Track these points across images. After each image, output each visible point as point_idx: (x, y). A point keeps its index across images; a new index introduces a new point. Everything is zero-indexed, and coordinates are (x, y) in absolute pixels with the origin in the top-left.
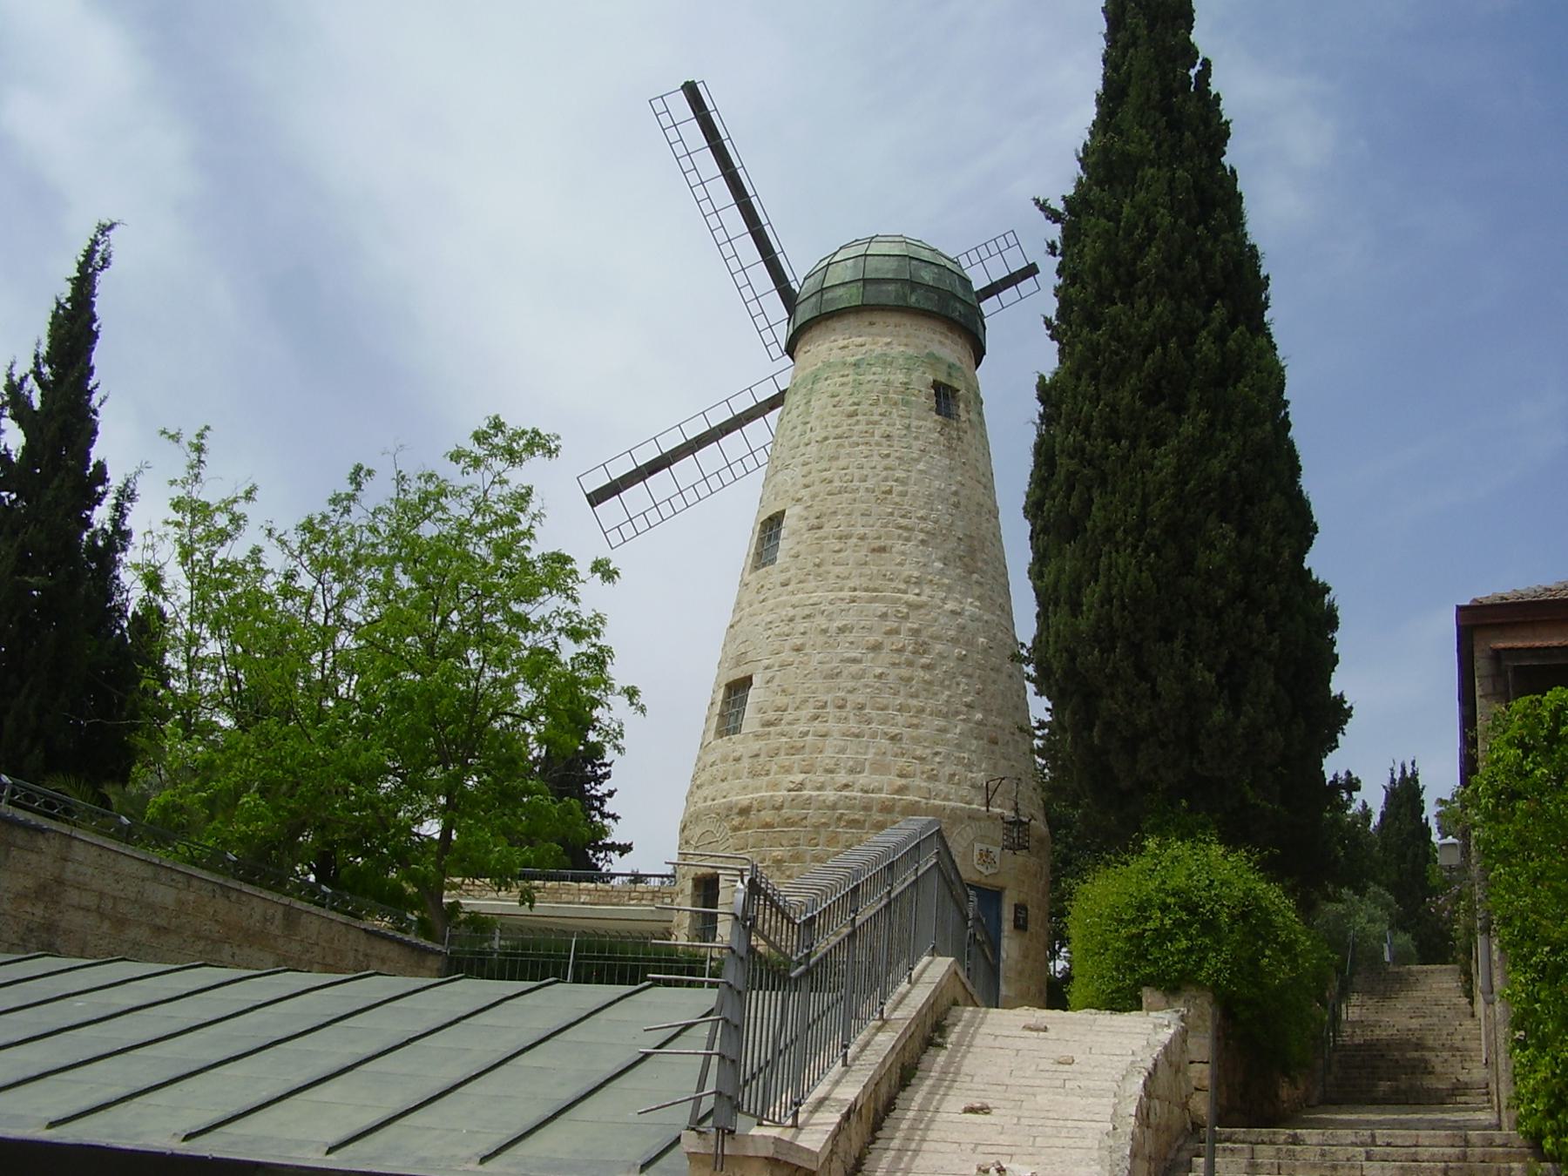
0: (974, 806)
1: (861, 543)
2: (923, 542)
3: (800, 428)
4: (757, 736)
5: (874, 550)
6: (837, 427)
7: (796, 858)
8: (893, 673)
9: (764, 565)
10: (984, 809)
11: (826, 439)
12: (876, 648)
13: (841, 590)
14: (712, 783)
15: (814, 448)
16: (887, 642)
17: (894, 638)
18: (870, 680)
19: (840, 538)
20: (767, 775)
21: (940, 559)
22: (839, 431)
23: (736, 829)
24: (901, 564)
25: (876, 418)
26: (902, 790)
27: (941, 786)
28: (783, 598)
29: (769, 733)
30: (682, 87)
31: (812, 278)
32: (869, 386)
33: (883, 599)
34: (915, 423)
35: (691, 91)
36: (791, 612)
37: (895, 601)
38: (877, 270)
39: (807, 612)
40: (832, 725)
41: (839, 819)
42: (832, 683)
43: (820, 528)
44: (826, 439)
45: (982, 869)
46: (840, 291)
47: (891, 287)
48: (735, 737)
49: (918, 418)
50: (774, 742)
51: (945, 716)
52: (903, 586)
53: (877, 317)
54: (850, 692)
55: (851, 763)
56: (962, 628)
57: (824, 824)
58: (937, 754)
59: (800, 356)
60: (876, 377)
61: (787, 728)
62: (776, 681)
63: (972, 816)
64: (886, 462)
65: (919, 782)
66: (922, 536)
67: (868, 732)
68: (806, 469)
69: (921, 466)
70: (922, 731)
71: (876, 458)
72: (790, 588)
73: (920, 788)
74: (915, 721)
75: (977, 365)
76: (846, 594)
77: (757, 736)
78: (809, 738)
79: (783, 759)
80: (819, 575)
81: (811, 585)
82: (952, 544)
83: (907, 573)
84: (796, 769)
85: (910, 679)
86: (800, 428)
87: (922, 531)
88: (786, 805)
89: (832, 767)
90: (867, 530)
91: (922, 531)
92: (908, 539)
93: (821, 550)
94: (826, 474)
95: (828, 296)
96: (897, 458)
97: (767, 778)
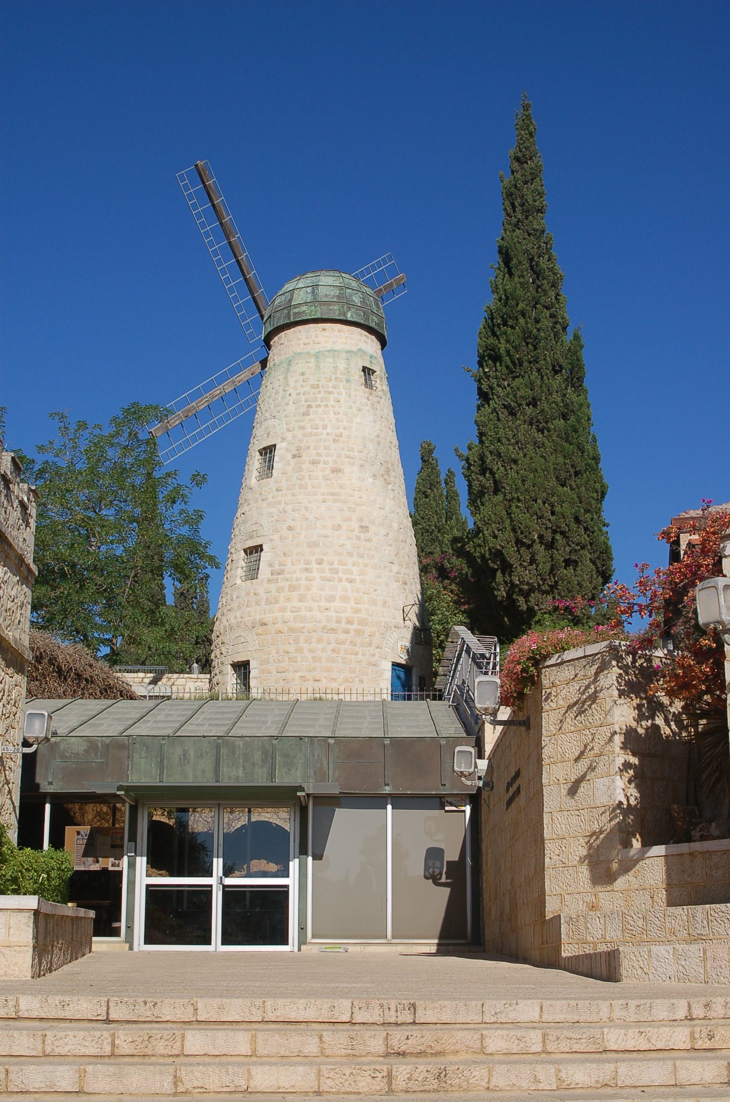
61: (288, 576)
69: (358, 420)
87: (360, 459)
92: (353, 464)
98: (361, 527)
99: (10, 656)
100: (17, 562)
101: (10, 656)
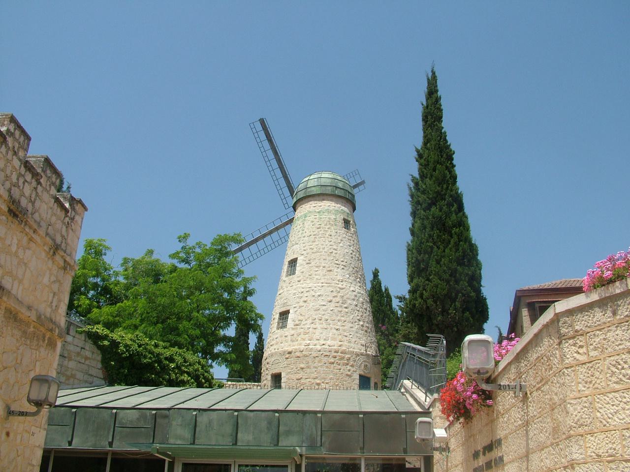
0: (362, 351)
1: (324, 268)
2: (343, 269)
3: (301, 232)
4: (293, 329)
5: (328, 271)
6: (313, 232)
7: (308, 367)
8: (336, 310)
9: (290, 275)
10: (365, 352)
11: (311, 235)
12: (330, 302)
13: (318, 283)
14: (277, 344)
15: (306, 238)
16: (334, 300)
17: (335, 298)
18: (329, 311)
19: (317, 267)
20: (297, 341)
21: (348, 274)
22: (315, 233)
23: (287, 358)
24: (336, 275)
25: (327, 229)
26: (340, 346)
27: (352, 345)
28: (299, 286)
29: (297, 328)
30: (259, 120)
31: (302, 184)
32: (323, 220)
33: (332, 286)
34: (339, 231)
35: (262, 122)
36: (302, 290)
37: (335, 287)
38: (325, 182)
39: (308, 290)
40: (317, 325)
41: (322, 355)
42: (318, 312)
43: (310, 263)
44: (311, 235)
45: (365, 371)
46: (313, 189)
47: (330, 188)
48: (285, 329)
49: (340, 230)
50: (299, 331)
51: (352, 323)
52: (338, 282)
53: (325, 197)
54: (323, 315)
55: (324, 337)
56: (356, 296)
57: (317, 356)
58: (351, 335)
59: (299, 210)
60: (326, 217)
61: (303, 327)
62: (298, 312)
63: (362, 355)
64: (331, 243)
65: (346, 343)
66: (343, 267)
67: (329, 328)
68: (304, 245)
70: (345, 327)
71: (327, 242)
72: (301, 282)
73: (346, 345)
74: (343, 324)
75: (354, 212)
76: (320, 285)
77: (293, 329)
78: (311, 329)
79: (302, 336)
80: (311, 278)
81: (308, 281)
82: (351, 269)
83: (338, 278)
84: (307, 340)
85: (341, 311)
86: (301, 232)
87: (342, 265)
88: (305, 350)
89: (318, 338)
90: (326, 265)
91: (342, 265)
92: (338, 268)
93: (311, 271)
94: (311, 247)
95: (309, 190)
96: (334, 242)
97: (297, 342)
99: (32, 329)
101: (32, 329)
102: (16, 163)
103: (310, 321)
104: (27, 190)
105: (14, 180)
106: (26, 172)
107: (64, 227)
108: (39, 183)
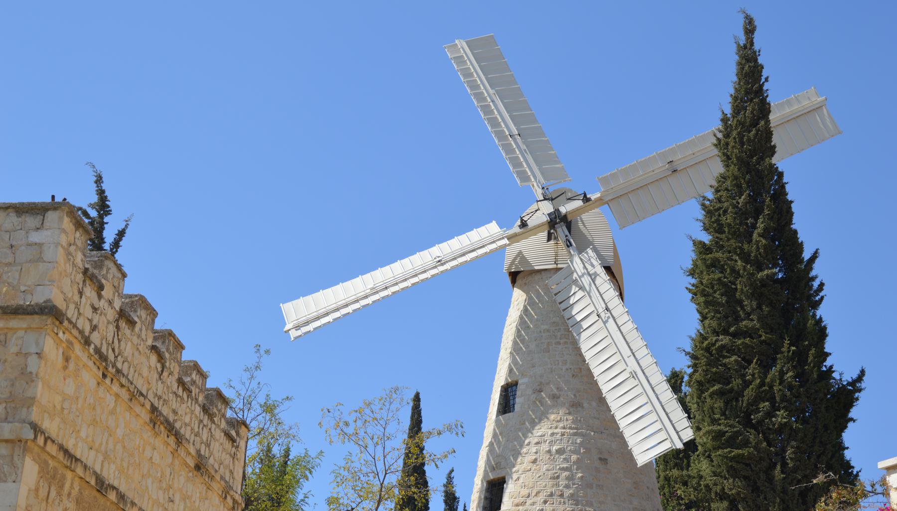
62: (521, 480)
98: (600, 459)
100: (221, 494)
102: (198, 409)
103: (541, 498)
104: (205, 435)
105: (196, 430)
106: (204, 415)
107: (231, 459)
108: (213, 422)
